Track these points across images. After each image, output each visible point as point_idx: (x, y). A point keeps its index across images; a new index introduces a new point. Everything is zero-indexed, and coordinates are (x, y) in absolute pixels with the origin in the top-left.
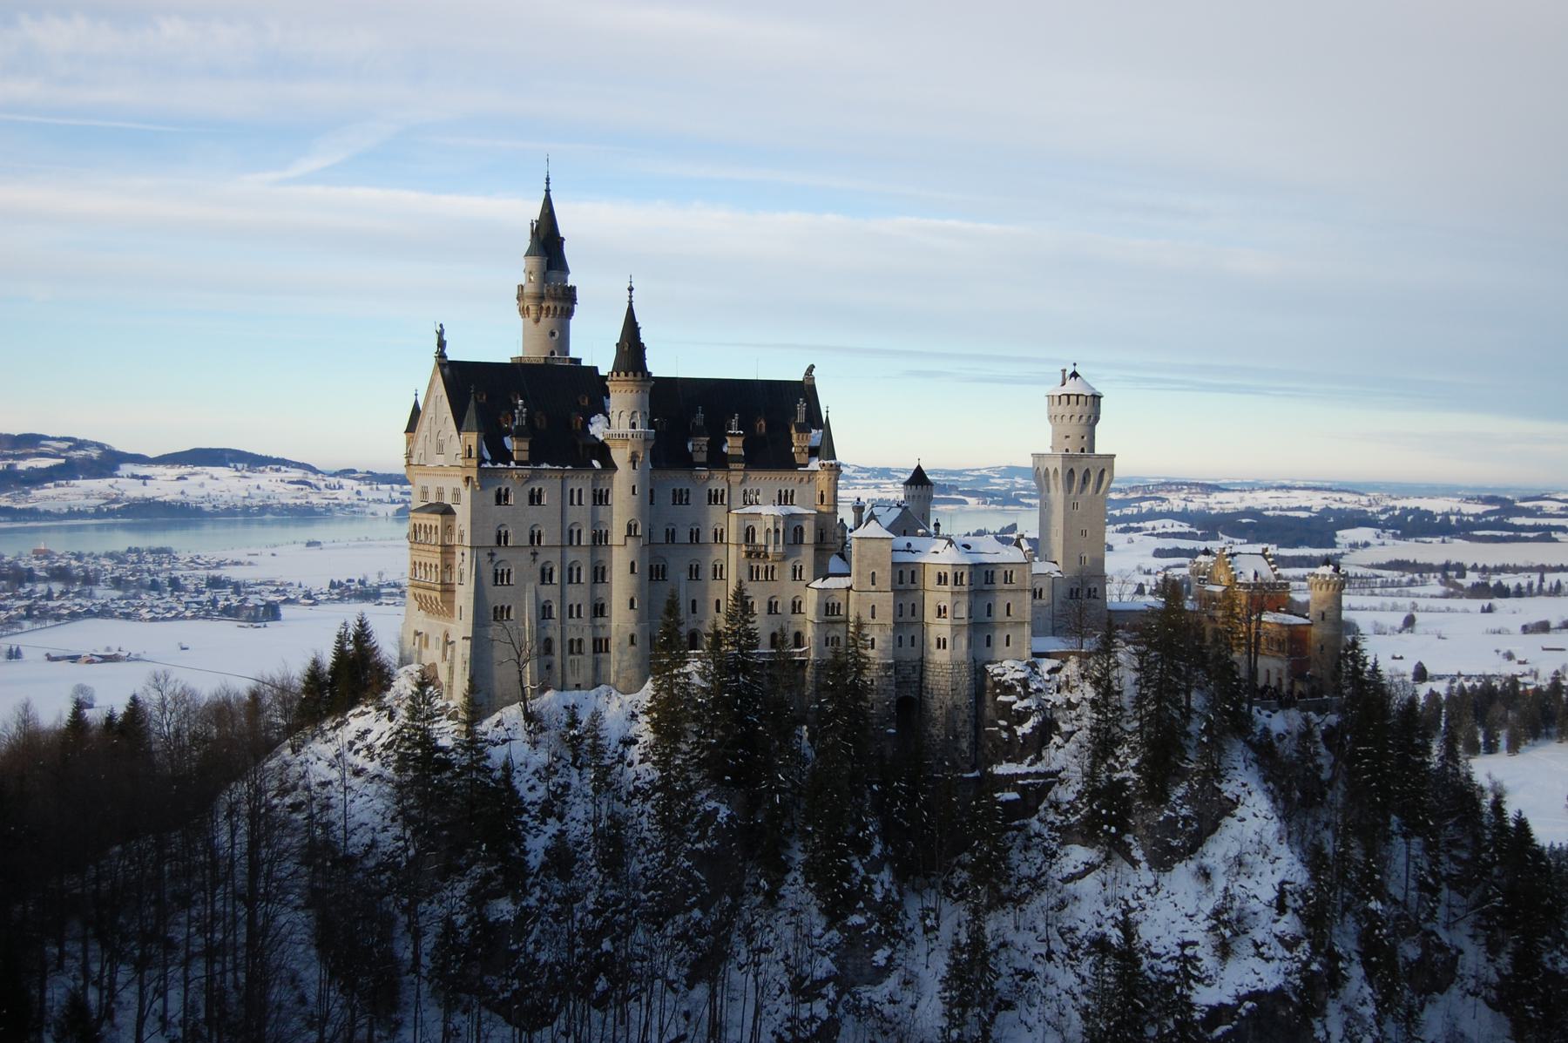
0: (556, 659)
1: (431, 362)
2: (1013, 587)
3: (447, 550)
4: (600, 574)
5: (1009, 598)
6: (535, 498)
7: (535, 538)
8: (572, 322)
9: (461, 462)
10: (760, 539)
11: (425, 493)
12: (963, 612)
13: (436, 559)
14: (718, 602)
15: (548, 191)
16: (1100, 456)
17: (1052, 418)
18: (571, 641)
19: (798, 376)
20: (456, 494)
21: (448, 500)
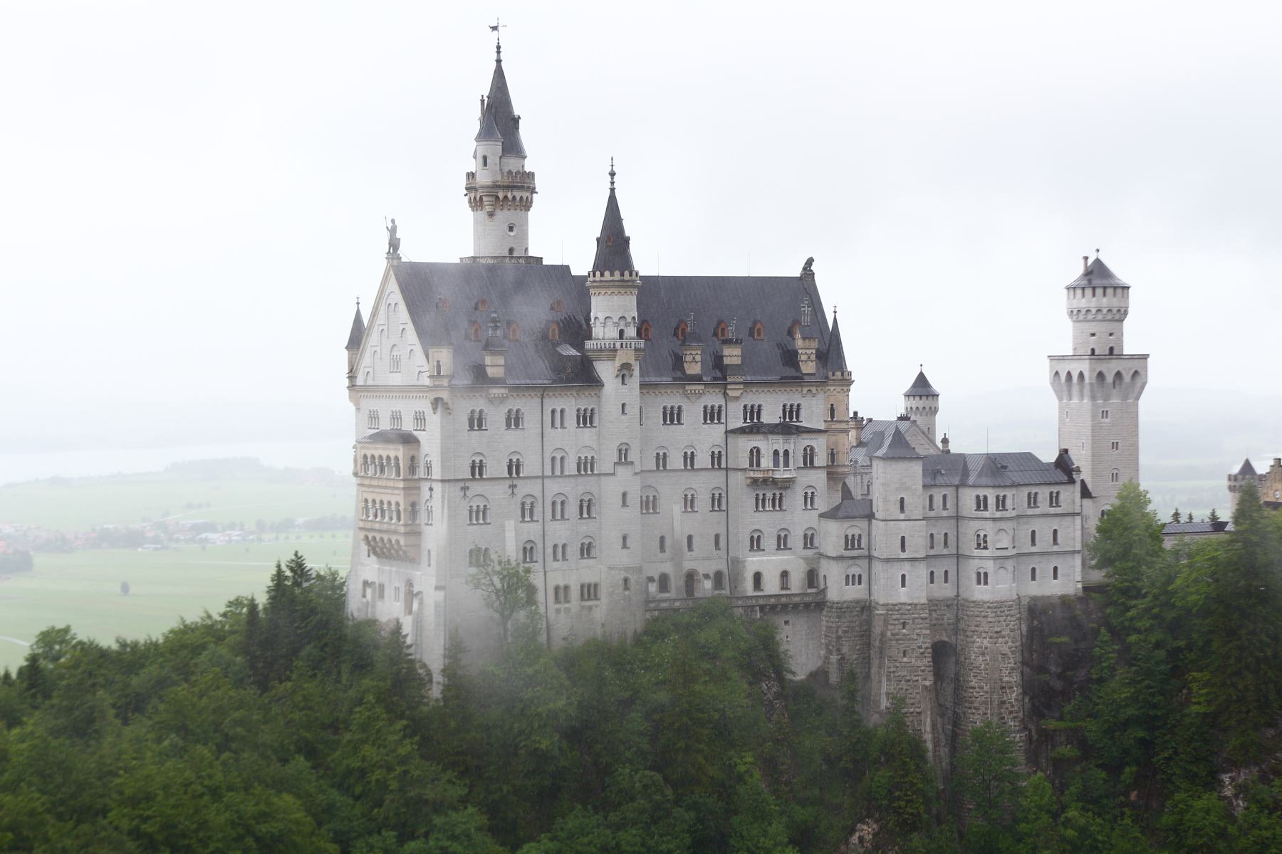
0: (542, 610)
1: (382, 264)
2: (1059, 510)
3: (412, 486)
4: (587, 508)
5: (1055, 524)
6: (514, 420)
7: (514, 468)
8: (532, 214)
9: (427, 382)
10: (766, 462)
11: (374, 417)
12: (1005, 541)
13: (398, 497)
14: (717, 537)
15: (499, 61)
16: (1132, 357)
17: (1075, 314)
18: (557, 588)
19: (796, 272)
20: (420, 418)
21: (408, 425)
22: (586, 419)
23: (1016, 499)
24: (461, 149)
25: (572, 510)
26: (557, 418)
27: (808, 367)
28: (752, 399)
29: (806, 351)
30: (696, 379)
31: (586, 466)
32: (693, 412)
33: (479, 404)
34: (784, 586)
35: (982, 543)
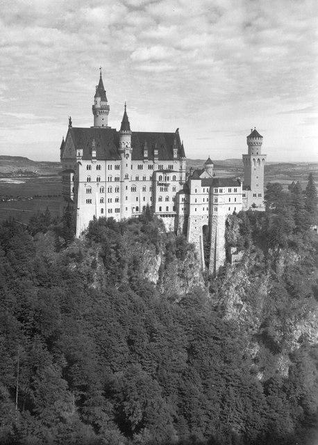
1: (66, 129)
5: (235, 196)
6: (98, 168)
7: (98, 180)
17: (248, 143)
22: (117, 168)
23: (225, 189)
24: (90, 100)
25: (113, 190)
26: (110, 168)
27: (175, 156)
28: (162, 163)
29: (175, 151)
30: (146, 158)
31: (117, 179)
32: (145, 166)
33: (89, 163)
34: (167, 210)
35: (216, 200)
